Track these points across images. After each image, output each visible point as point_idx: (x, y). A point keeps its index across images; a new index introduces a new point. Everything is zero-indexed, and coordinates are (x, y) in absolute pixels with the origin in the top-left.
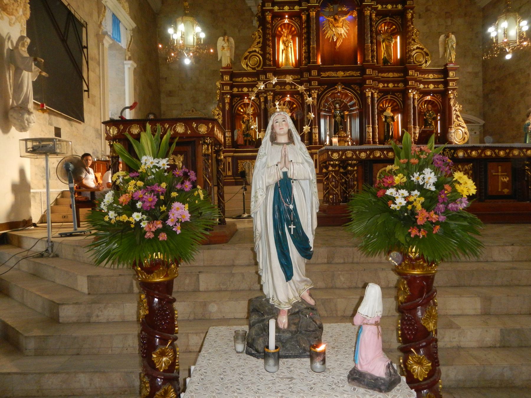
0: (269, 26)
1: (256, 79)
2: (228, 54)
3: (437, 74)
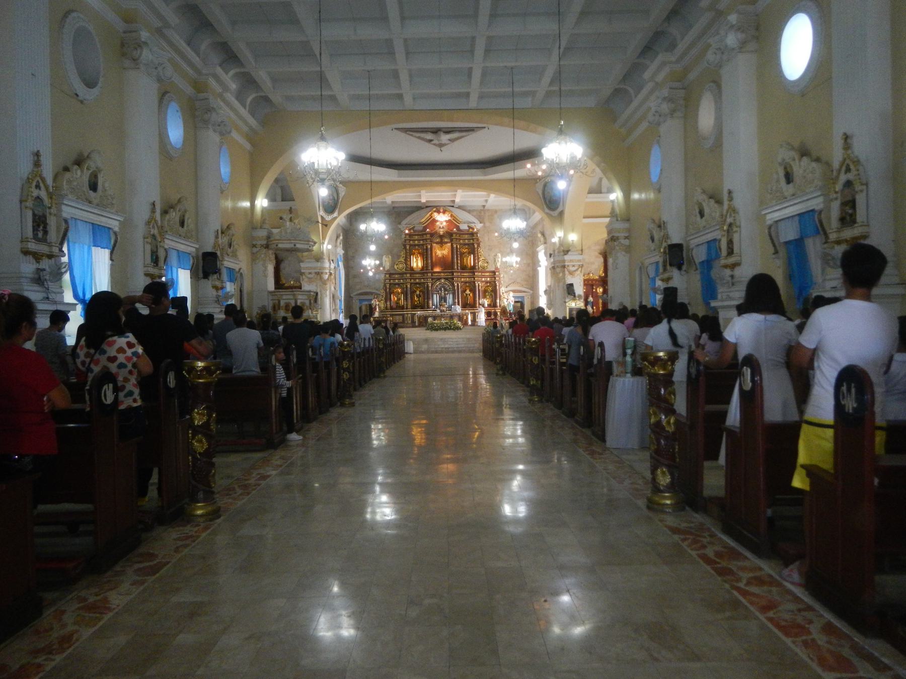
0: (408, 251)
2: (388, 264)
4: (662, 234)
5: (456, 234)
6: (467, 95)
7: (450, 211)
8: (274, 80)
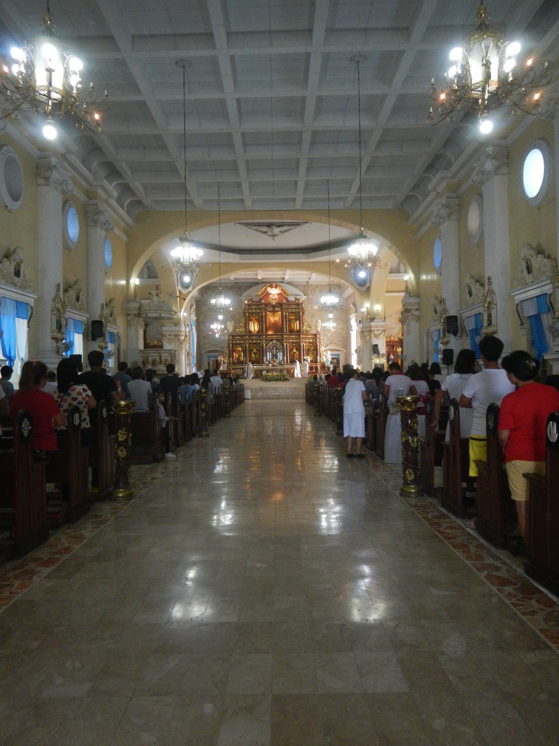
2: (231, 328)
4: (442, 308)
5: (286, 304)
6: (294, 200)
7: (281, 286)
8: (145, 188)
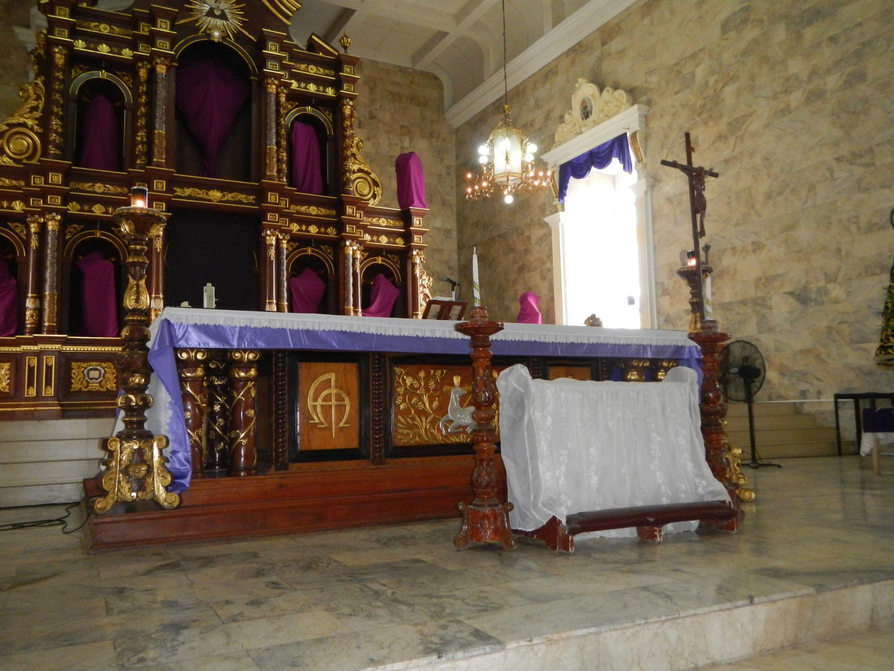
0: (60, 75)
1: (23, 183)
3: (392, 219)
